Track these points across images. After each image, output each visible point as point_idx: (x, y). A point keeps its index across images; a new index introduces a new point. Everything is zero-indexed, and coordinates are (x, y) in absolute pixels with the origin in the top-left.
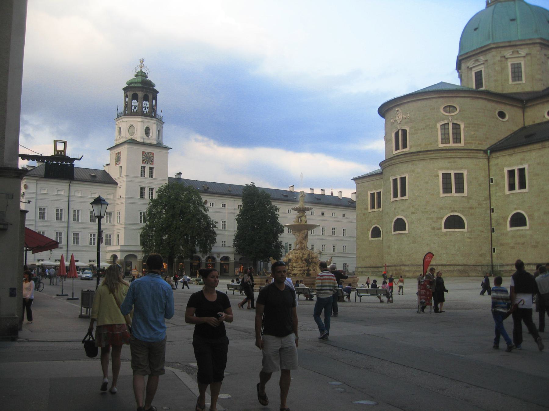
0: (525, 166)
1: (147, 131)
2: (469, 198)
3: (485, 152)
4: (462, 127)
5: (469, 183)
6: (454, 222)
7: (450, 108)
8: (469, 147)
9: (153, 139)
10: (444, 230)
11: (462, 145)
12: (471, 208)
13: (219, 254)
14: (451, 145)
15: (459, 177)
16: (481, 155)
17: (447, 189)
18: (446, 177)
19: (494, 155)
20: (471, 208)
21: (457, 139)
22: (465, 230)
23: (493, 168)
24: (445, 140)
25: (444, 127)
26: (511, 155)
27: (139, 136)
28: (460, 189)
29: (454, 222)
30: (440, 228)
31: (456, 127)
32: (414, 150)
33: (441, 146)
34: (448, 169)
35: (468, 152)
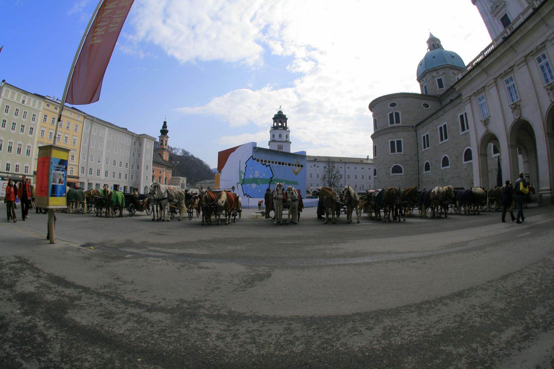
0: (428, 133)
1: (280, 136)
2: (405, 155)
3: (413, 127)
4: (400, 114)
5: (405, 145)
6: (397, 170)
7: (393, 105)
8: (405, 125)
9: (284, 138)
10: (392, 174)
11: (400, 124)
12: (406, 161)
13: (311, 190)
14: (395, 124)
15: (399, 142)
16: (411, 129)
17: (393, 150)
18: (392, 143)
19: (418, 128)
20: (406, 161)
21: (398, 122)
22: (402, 174)
23: (418, 136)
24: (392, 122)
25: (391, 115)
26: (423, 127)
27: (277, 138)
28: (399, 150)
29: (397, 170)
30: (389, 174)
31: (397, 114)
32: (379, 129)
33: (390, 125)
34: (393, 138)
35: (405, 128)
